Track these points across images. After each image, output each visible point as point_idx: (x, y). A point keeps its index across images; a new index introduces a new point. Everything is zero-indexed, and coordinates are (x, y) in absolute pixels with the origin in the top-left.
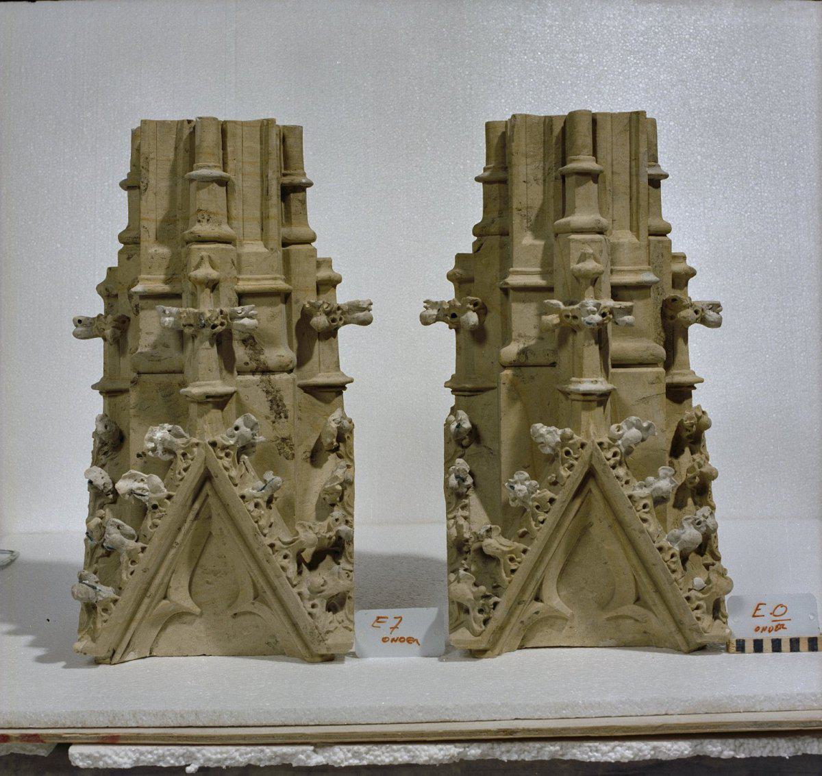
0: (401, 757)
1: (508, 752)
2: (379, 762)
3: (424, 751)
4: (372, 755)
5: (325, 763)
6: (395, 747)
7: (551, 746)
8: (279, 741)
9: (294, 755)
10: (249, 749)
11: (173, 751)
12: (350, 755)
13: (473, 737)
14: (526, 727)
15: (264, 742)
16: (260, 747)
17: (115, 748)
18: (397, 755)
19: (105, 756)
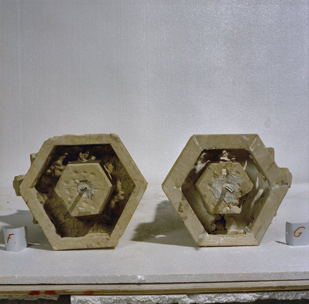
0: (231, 299)
1: (282, 295)
2: (221, 302)
3: (243, 296)
4: (217, 298)
5: (194, 302)
6: (228, 295)
7: (302, 293)
8: (172, 293)
9: (179, 299)
10: (158, 296)
11: (121, 298)
12: (207, 299)
13: (265, 290)
14: (290, 285)
15: (165, 293)
16: (163, 296)
17: (93, 297)
18: (229, 298)
19: (88, 301)
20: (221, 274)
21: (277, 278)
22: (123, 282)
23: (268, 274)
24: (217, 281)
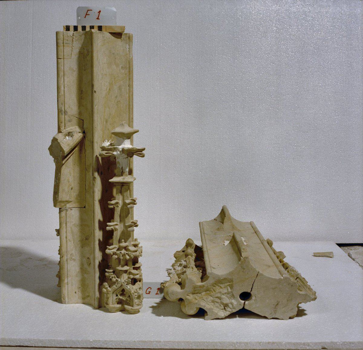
20: (188, 341)
21: (242, 347)
22: (95, 347)
23: (234, 344)
24: (185, 348)
